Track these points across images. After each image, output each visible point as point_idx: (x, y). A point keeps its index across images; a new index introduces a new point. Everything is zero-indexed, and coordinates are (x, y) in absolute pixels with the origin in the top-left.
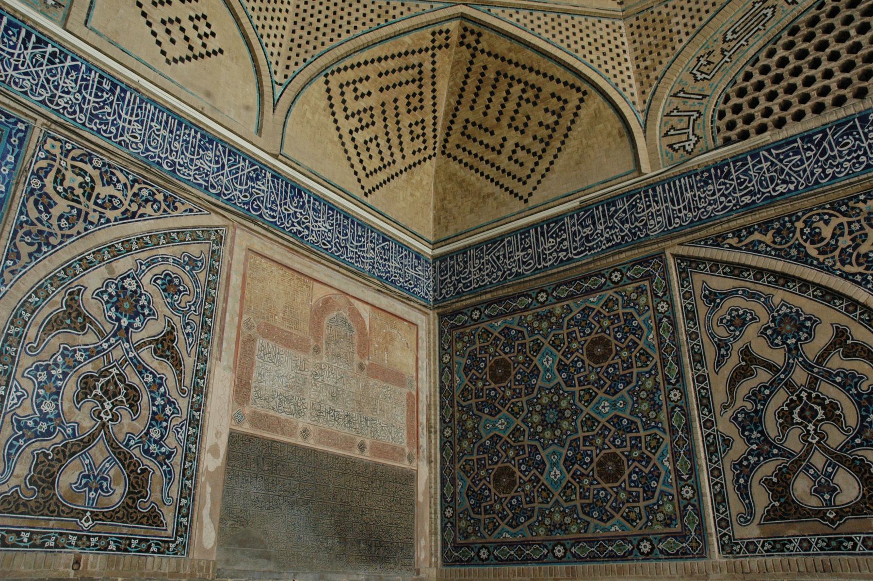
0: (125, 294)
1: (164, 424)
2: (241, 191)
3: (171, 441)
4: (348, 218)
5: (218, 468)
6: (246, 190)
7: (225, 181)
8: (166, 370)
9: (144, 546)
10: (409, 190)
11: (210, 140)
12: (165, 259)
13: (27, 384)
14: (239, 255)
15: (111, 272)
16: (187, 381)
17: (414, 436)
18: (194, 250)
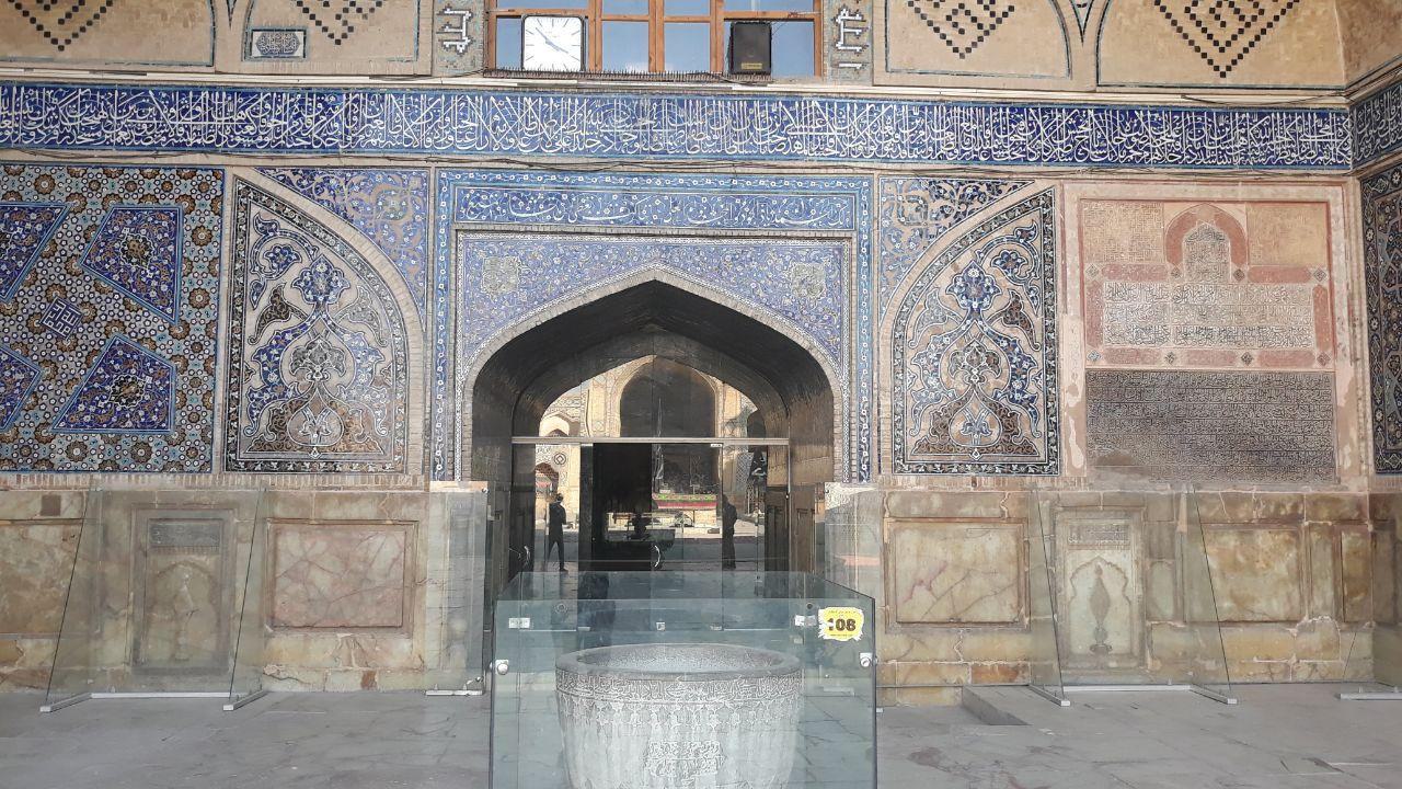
0: (971, 282)
1: (1024, 376)
2: (1062, 146)
3: (1032, 389)
4: (1202, 114)
5: (1078, 404)
6: (1067, 142)
7: (1043, 143)
8: (1019, 334)
9: (1023, 469)
10: (1294, 36)
11: (1018, 109)
12: (1000, 241)
13: (915, 369)
14: (1071, 209)
15: (956, 268)
16: (1039, 338)
17: (1327, 332)
18: (1025, 222)
